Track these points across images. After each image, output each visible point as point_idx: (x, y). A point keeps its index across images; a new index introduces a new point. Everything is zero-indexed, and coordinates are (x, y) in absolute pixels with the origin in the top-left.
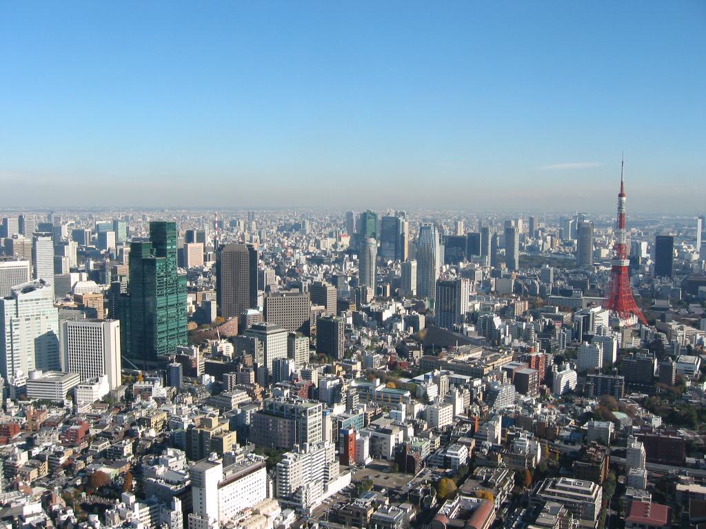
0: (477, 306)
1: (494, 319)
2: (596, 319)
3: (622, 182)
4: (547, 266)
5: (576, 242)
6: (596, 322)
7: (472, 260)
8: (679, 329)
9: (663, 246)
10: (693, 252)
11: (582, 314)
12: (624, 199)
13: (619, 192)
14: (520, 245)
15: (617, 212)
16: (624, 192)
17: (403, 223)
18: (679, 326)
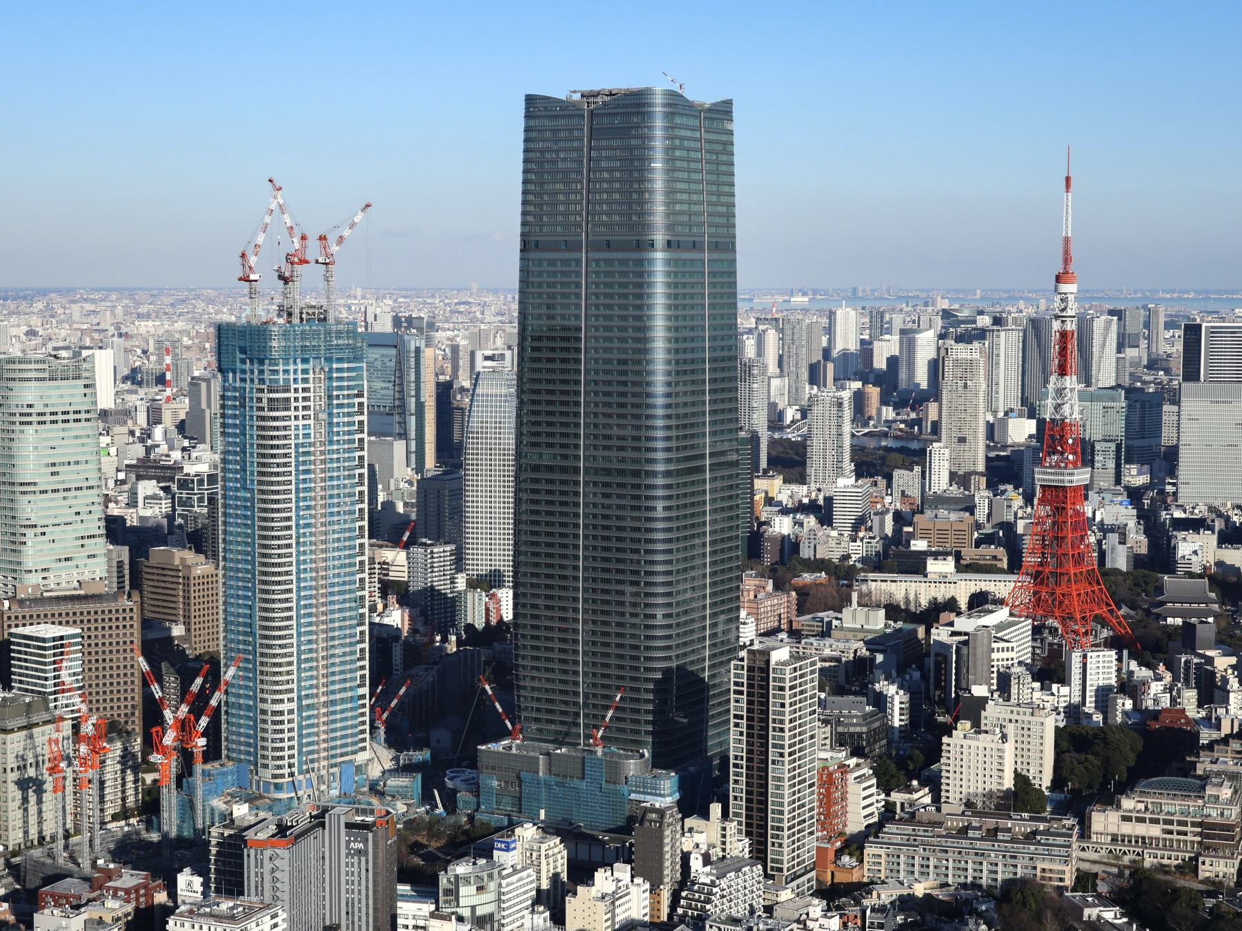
2: (994, 645)
3: (1067, 240)
6: (995, 656)
11: (954, 634)
16: (1071, 268)
17: (418, 350)
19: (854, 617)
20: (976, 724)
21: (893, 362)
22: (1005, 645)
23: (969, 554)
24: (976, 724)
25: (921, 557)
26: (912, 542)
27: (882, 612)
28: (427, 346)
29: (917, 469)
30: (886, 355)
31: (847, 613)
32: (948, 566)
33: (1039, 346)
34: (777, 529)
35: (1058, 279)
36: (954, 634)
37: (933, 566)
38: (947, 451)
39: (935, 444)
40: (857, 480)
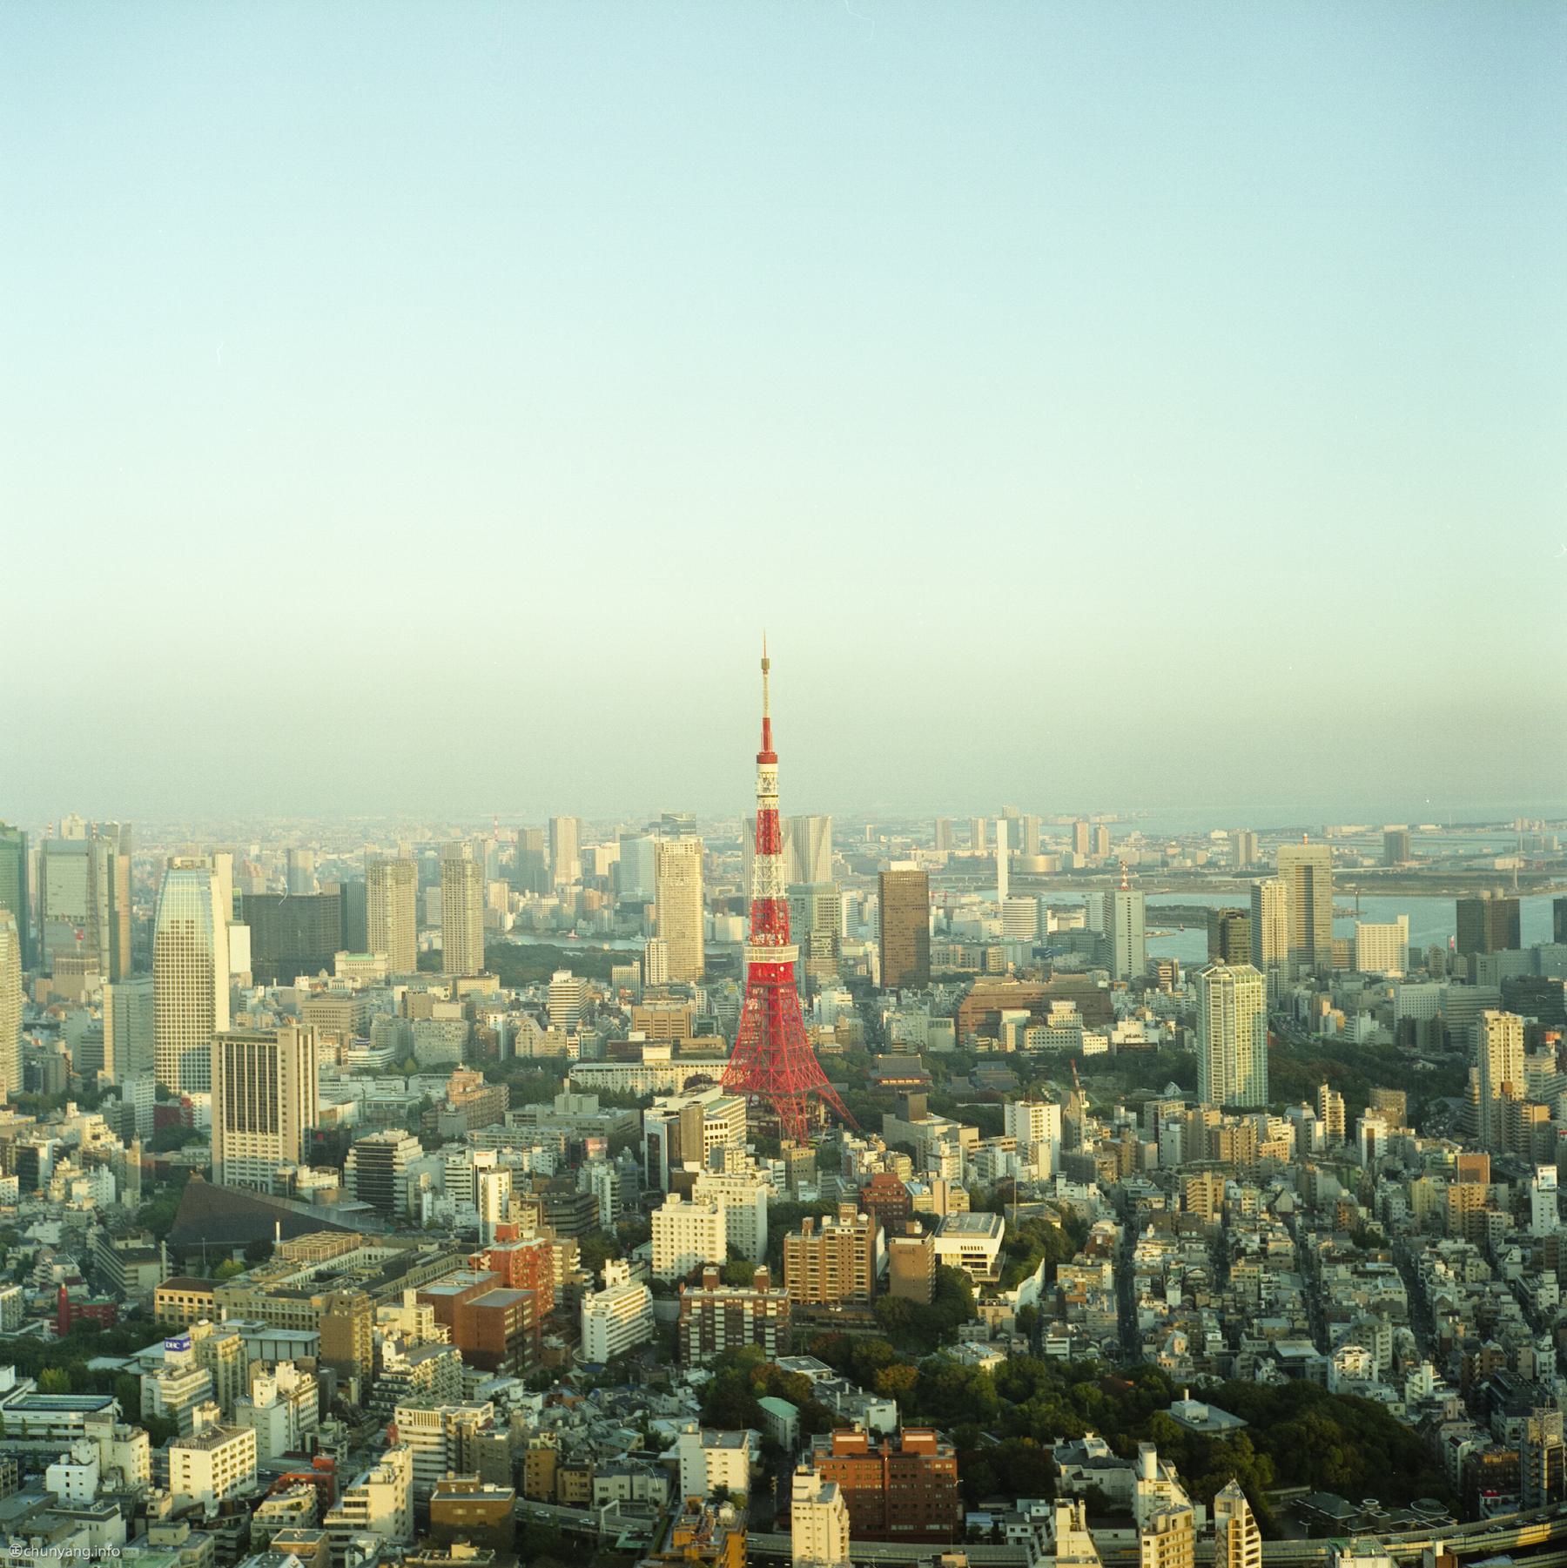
7: (339, 966)
18: (945, 1129)
19: (566, 1104)
20: (687, 1196)
21: (615, 868)
23: (688, 1044)
24: (687, 1196)
25: (640, 1044)
27: (596, 1098)
28: (122, 853)
29: (637, 964)
31: (559, 1099)
32: (665, 1053)
36: (667, 1114)
37: (649, 1054)
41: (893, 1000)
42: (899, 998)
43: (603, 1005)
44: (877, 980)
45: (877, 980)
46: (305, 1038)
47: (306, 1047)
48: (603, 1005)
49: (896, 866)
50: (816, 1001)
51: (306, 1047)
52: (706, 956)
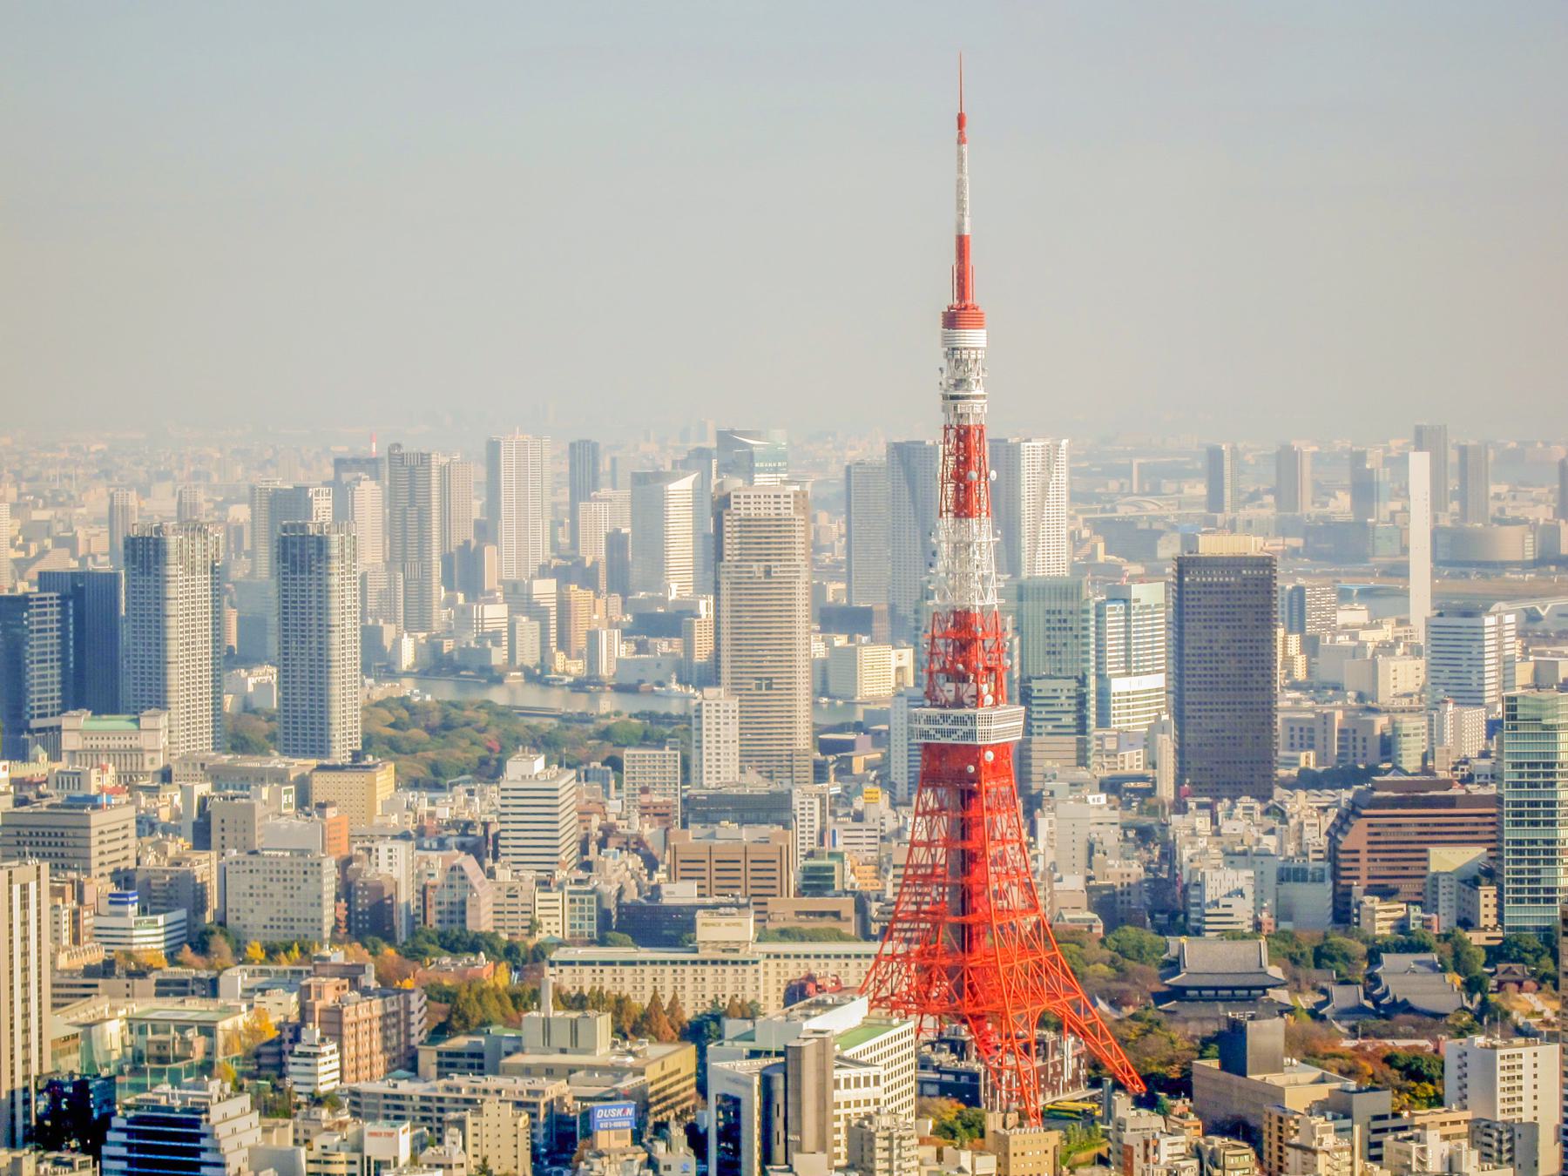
0: (113, 1037)
1: (216, 1113)
2: (841, 1074)
3: (962, 244)
4: (539, 764)
5: (705, 607)
7: (69, 742)
8: (1321, 1108)
9: (1226, 619)
10: (1387, 648)
12: (974, 339)
13: (948, 299)
14: (371, 639)
15: (941, 419)
16: (979, 295)
18: (1322, 1092)
21: (615, 542)
22: (862, 1072)
26: (665, 889)
30: (605, 528)
33: (914, 502)
34: (384, 868)
35: (952, 320)
37: (711, 931)
38: (734, 704)
39: (710, 692)
40: (547, 766)
41: (1202, 823)
42: (1214, 820)
43: (608, 831)
44: (1167, 791)
45: (1167, 791)
46: (24, 887)
47: (25, 906)
48: (608, 831)
49: (1211, 545)
50: (1043, 825)
51: (25, 906)
52: (818, 729)
